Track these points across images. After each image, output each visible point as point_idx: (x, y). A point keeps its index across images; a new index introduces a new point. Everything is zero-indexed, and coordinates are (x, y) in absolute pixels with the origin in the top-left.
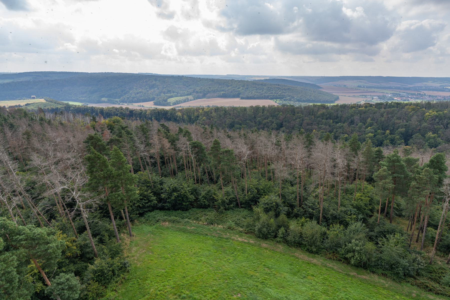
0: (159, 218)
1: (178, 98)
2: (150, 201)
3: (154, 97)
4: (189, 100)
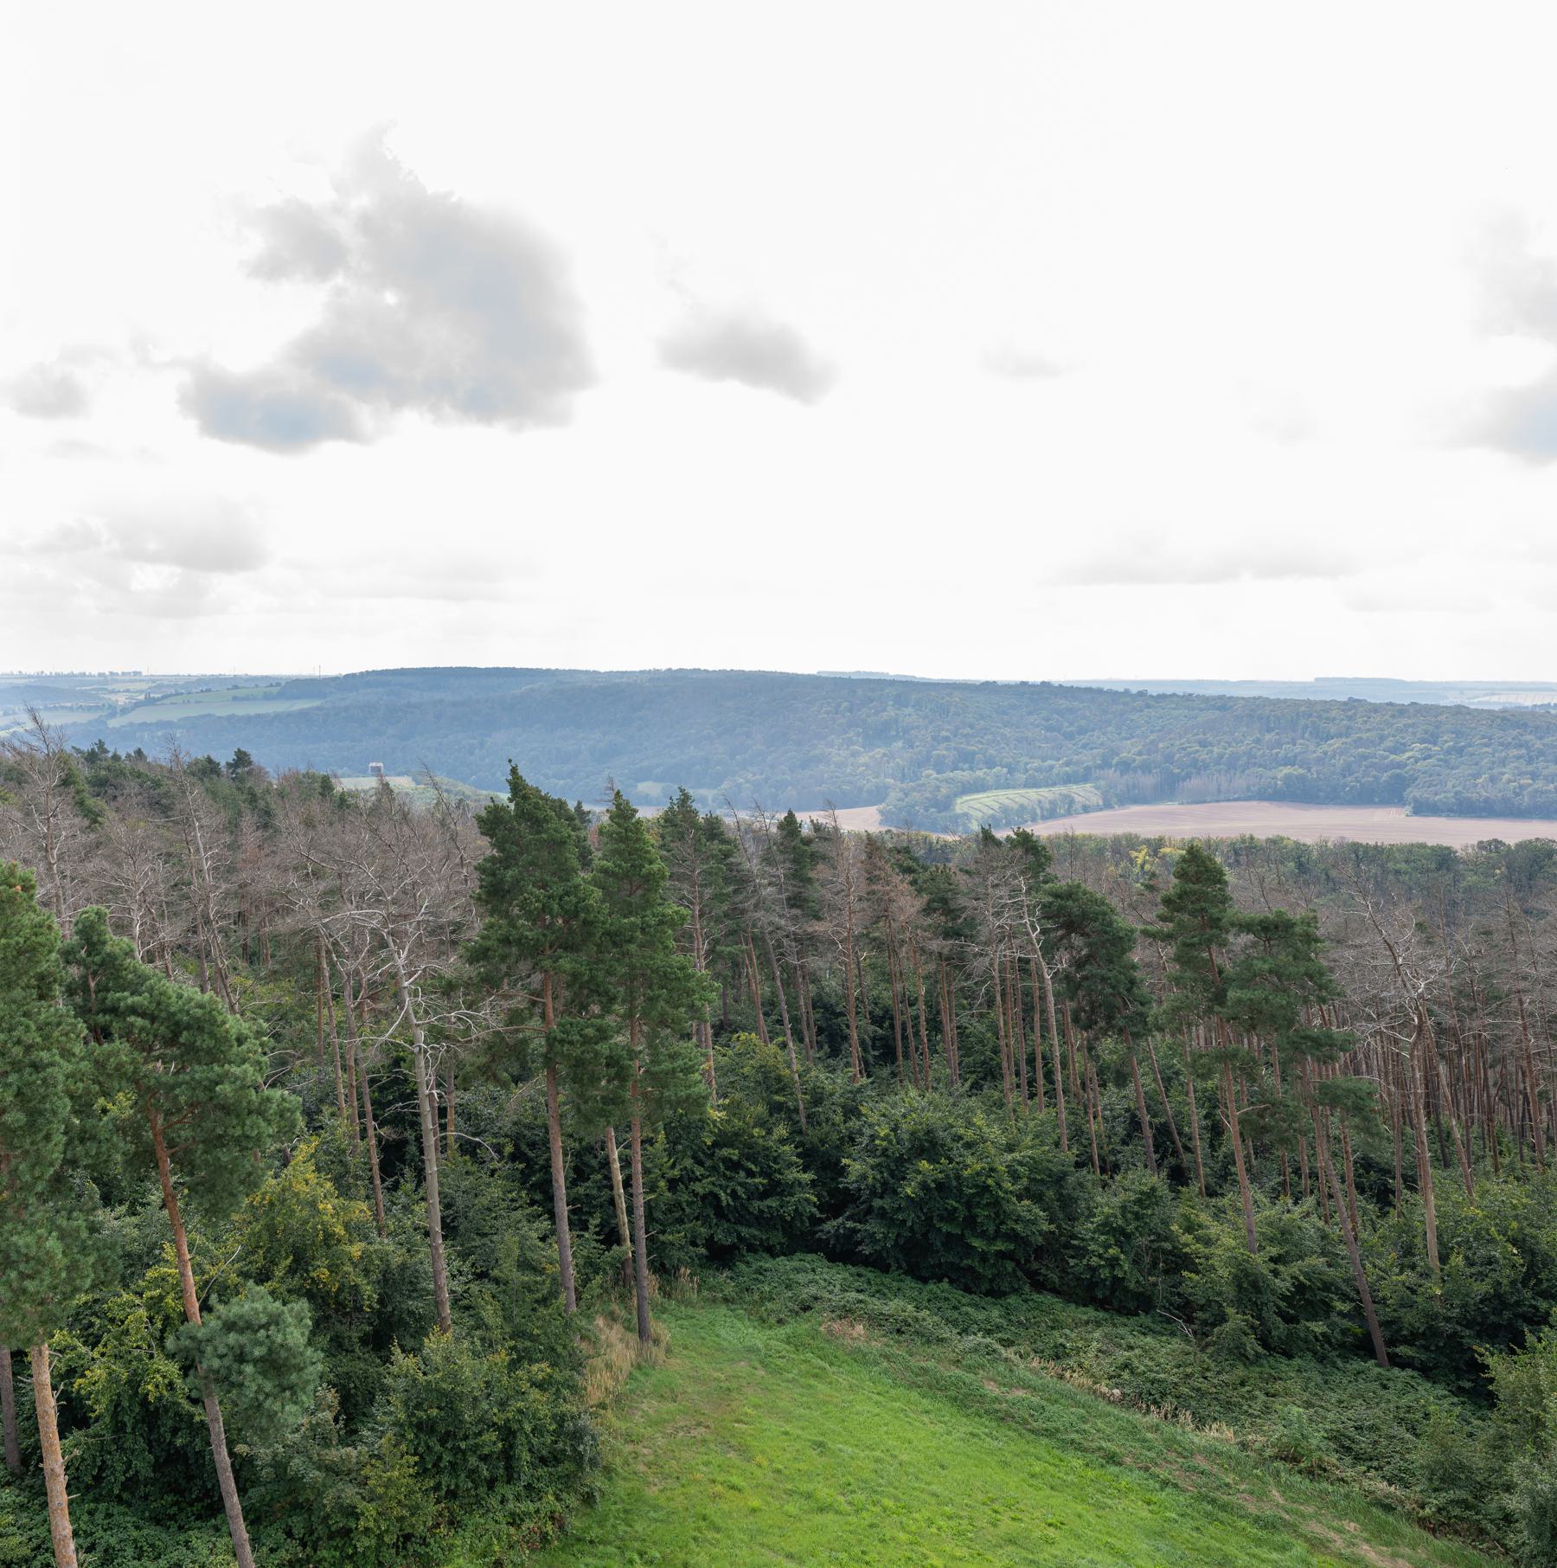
0: (813, 1290)
1: (1011, 793)
2: (776, 1188)
3: (886, 787)
4: (1078, 806)
